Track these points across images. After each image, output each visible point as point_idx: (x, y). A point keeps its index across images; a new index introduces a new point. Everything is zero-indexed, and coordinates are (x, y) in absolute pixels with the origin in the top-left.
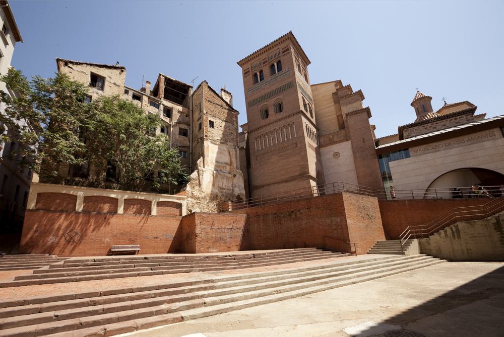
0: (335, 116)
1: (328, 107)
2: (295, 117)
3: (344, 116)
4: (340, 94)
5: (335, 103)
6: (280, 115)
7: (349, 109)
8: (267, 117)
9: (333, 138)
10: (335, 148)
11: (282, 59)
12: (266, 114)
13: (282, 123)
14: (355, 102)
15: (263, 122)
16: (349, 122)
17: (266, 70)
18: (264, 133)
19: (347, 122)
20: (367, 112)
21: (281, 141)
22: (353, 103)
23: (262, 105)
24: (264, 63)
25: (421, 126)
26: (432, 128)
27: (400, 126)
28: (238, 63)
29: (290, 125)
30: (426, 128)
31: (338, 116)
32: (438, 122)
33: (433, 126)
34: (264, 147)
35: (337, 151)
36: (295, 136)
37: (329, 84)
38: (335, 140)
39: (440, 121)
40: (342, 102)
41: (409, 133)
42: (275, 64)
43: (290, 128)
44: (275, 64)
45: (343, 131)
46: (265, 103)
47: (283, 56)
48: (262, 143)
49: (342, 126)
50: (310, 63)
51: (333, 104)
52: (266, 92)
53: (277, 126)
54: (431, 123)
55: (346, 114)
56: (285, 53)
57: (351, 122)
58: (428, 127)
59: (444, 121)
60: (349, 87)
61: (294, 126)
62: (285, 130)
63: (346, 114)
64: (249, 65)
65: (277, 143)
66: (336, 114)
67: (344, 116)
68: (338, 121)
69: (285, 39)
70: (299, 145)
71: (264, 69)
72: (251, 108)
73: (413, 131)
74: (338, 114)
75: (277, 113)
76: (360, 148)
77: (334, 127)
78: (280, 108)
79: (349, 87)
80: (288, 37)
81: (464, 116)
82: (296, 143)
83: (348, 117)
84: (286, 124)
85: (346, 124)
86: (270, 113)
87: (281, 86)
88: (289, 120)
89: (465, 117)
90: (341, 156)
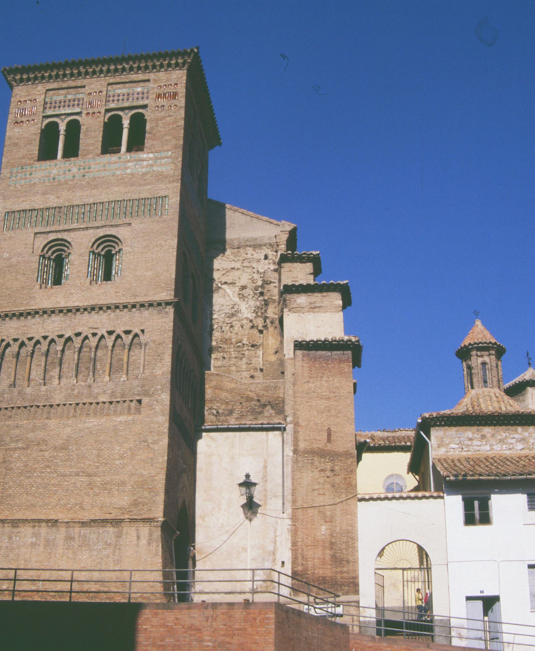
6: (104, 293)
8: (57, 281)
18: (37, 337)
23: (52, 237)
42: (126, 123)
44: (126, 123)
46: (59, 236)
50: (220, 144)
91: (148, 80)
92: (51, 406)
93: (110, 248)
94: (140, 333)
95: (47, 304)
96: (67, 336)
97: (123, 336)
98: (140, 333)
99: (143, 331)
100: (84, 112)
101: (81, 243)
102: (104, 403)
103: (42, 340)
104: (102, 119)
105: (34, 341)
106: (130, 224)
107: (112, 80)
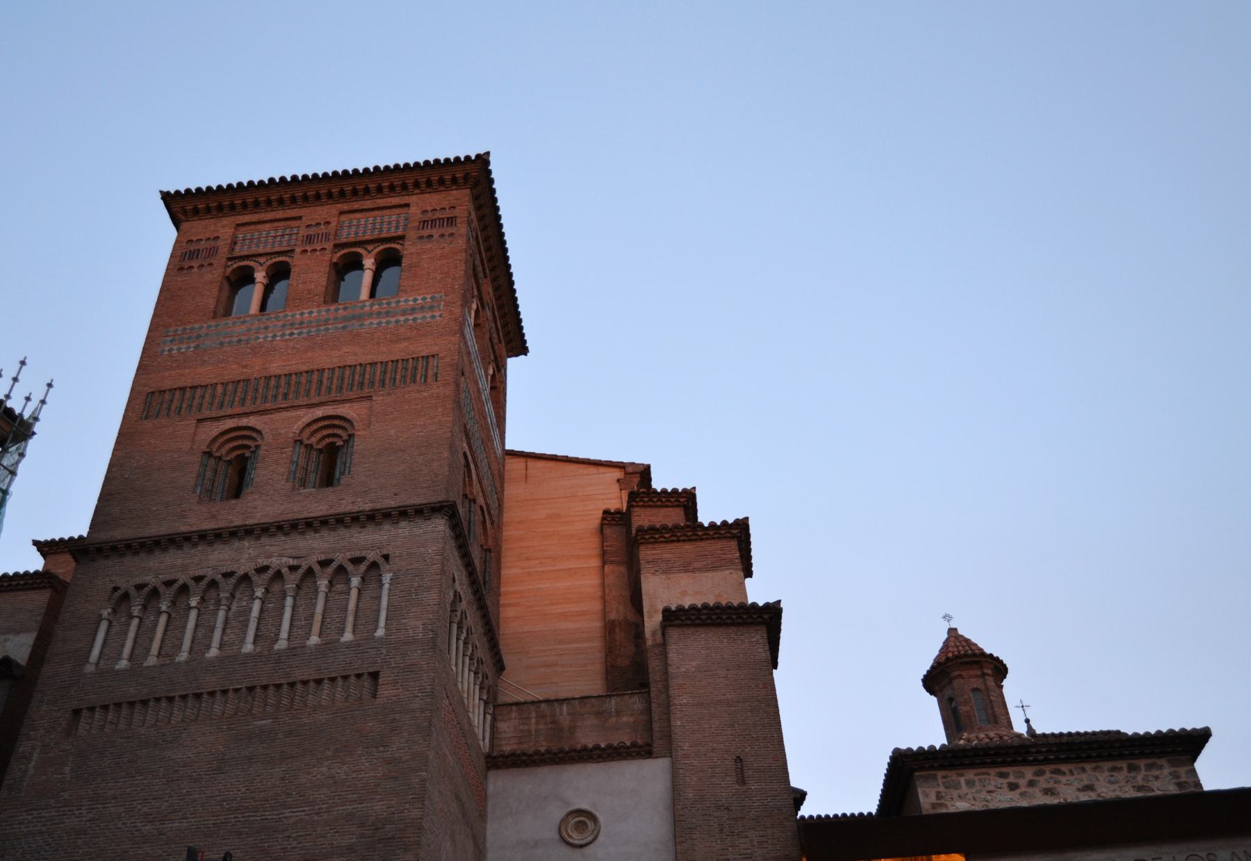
0: (597, 624)
1: (571, 572)
2: (404, 529)
3: (652, 621)
4: (643, 518)
5: (604, 563)
7: (684, 594)
9: (573, 729)
10: (583, 786)
11: (409, 250)
12: (235, 468)
13: (315, 546)
14: (714, 568)
15: (199, 519)
16: (673, 656)
17: (311, 272)
18: (183, 578)
19: (664, 655)
20: (768, 619)
21: (282, 644)
22: (700, 570)
23: (230, 424)
24: (309, 239)
25: (993, 771)
26: (1036, 791)
27: (903, 747)
28: (168, 198)
29: (363, 567)
30: (1013, 787)
31: (610, 628)
32: (1064, 768)
33: (1043, 782)
34: (152, 660)
35: (584, 806)
36: (380, 632)
37: (592, 470)
38: (587, 737)
39: (1072, 766)
40: (646, 553)
41: (939, 796)
43: (355, 581)
45: (636, 703)
46: (244, 422)
47: (421, 237)
48: (144, 635)
49: (631, 664)
50: (524, 350)
51: (595, 563)
52: (275, 367)
53: (278, 552)
54: (1035, 769)
55: (666, 611)
56: (436, 232)
57: (690, 656)
58: (1022, 782)
59: (1088, 766)
60: (686, 500)
61: (387, 578)
62: (323, 584)
63: (666, 611)
64: (223, 228)
65: (248, 647)
66: (604, 613)
67: (652, 621)
68: (610, 650)
69: (447, 177)
70: (385, 692)
71: (298, 262)
72: (148, 424)
73: (957, 786)
74: (613, 616)
75: (304, 484)
76: (718, 808)
77: (582, 676)
78: (328, 457)
79: (686, 500)
80: (466, 177)
81: (1162, 762)
82: (375, 676)
83: (674, 634)
84: (340, 558)
85: (654, 665)
86: (260, 473)
87: (369, 359)
88: (366, 540)
89: (1167, 771)
90: (601, 838)
91: (407, 205)
92: (198, 696)
93: (331, 440)
94: (381, 561)
95: (207, 525)
96: (241, 572)
97: (350, 567)
98: (381, 561)
99: (386, 557)
100: (298, 250)
101: (282, 427)
102: (305, 683)
103: (191, 583)
104: (327, 256)
105: (176, 586)
106: (369, 398)
107: (345, 207)
